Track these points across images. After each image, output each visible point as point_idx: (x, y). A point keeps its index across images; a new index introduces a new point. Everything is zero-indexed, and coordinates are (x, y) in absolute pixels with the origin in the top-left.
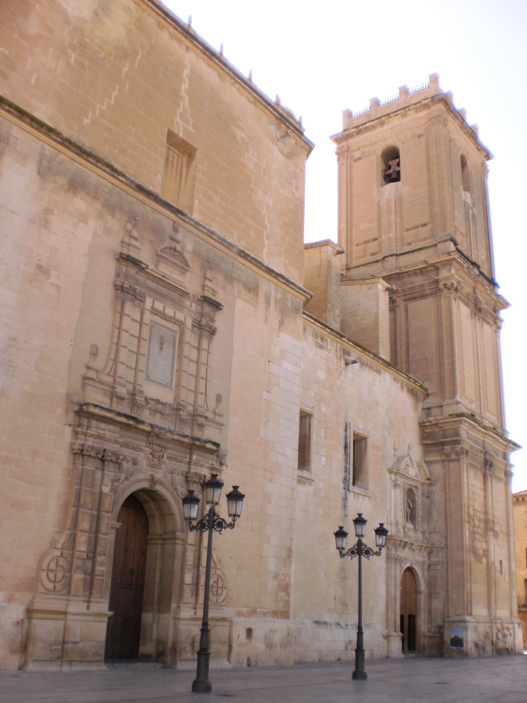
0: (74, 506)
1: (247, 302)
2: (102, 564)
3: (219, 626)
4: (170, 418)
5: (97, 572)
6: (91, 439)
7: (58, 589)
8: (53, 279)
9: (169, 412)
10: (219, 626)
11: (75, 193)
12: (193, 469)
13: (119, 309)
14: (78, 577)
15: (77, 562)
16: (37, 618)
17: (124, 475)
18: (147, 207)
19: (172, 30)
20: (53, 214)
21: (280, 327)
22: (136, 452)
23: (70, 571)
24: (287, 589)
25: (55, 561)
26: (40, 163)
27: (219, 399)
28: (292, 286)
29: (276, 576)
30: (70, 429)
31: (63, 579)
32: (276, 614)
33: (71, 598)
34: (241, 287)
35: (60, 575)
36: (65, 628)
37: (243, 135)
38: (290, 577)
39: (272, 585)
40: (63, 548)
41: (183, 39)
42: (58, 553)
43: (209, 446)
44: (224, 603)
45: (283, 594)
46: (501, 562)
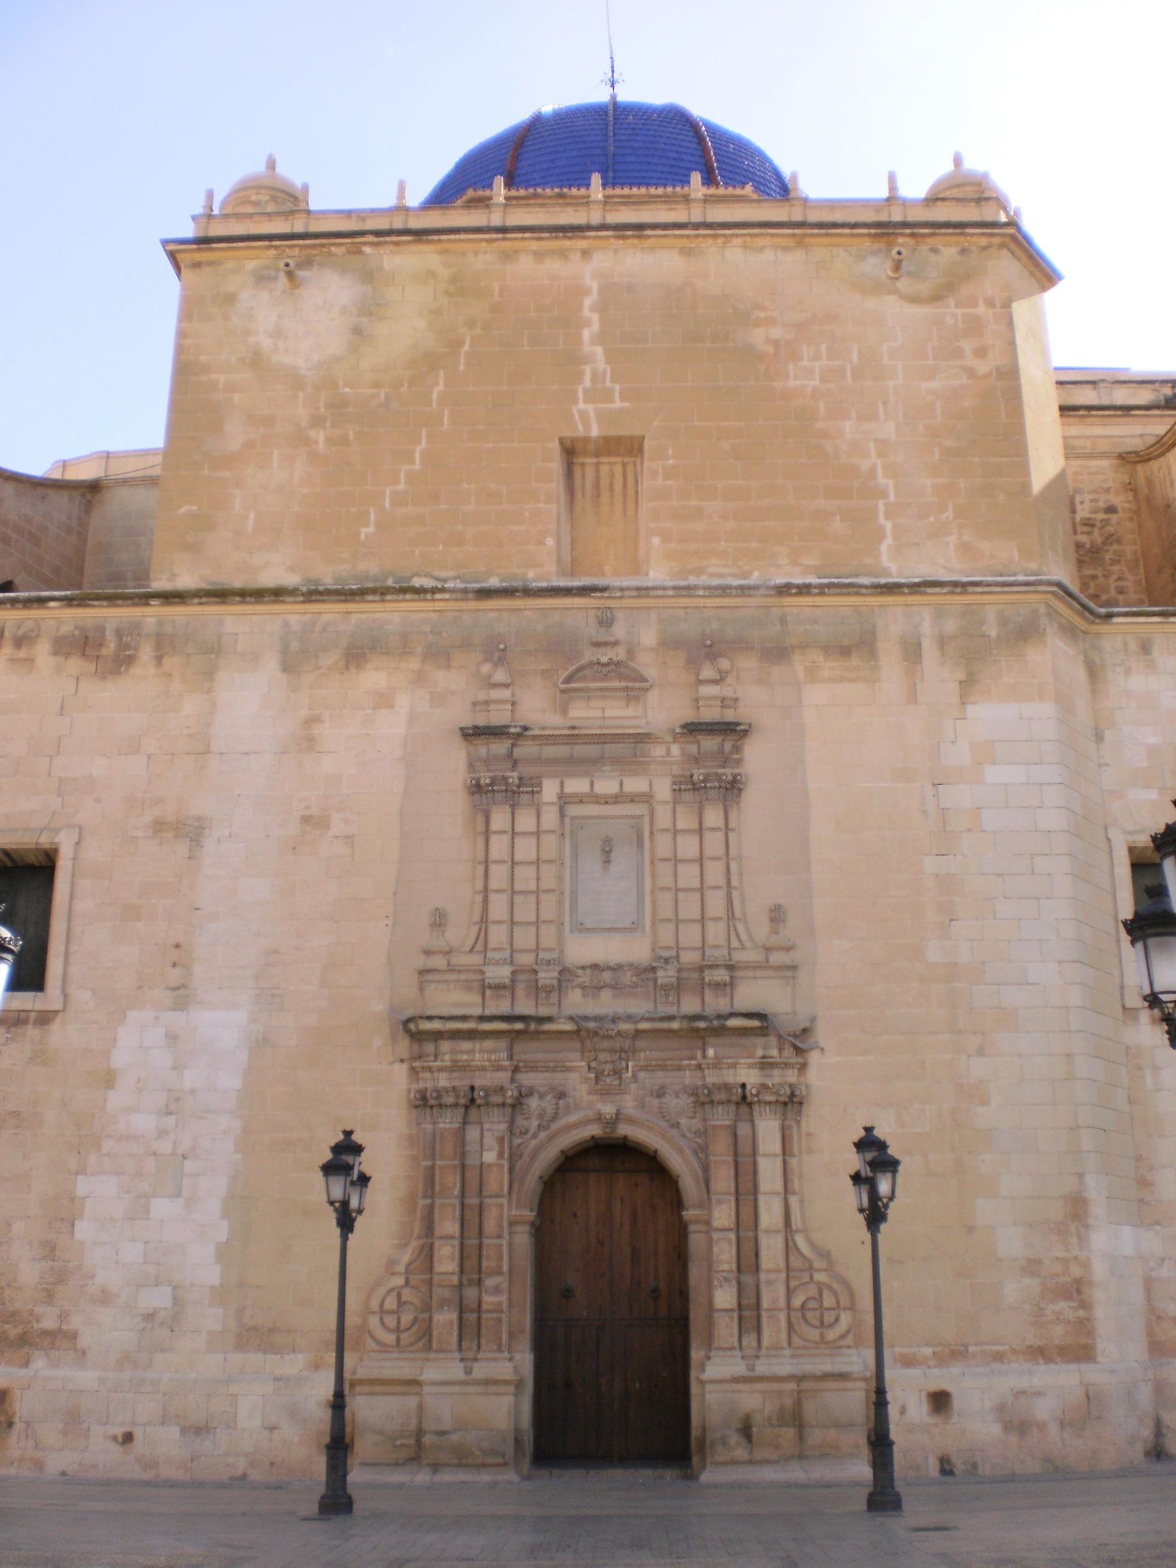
0: (424, 1197)
1: (842, 680)
2: (497, 1290)
3: (830, 1390)
4: (639, 989)
5: (484, 1307)
6: (443, 1075)
7: (403, 1342)
8: (337, 826)
9: (634, 979)
10: (830, 1390)
11: (359, 666)
12: (712, 1078)
13: (481, 827)
14: (445, 1318)
15: (439, 1293)
16: (361, 1394)
17: (535, 1123)
18: (527, 613)
19: (534, 245)
20: (323, 722)
22: (559, 1075)
23: (427, 1308)
24: (1079, 1292)
25: (394, 1294)
26: (285, 650)
27: (777, 915)
28: (980, 589)
29: (1032, 1267)
30: (405, 1067)
31: (413, 1324)
32: (1040, 1353)
33: (432, 1355)
34: (817, 657)
35: (406, 1319)
36: (421, 1408)
37: (776, 332)
38: (1086, 1264)
39: (1015, 1289)
40: (408, 1271)
41: (567, 243)
42: (399, 1281)
43: (733, 1022)
44: (849, 1341)
45: (1062, 1305)
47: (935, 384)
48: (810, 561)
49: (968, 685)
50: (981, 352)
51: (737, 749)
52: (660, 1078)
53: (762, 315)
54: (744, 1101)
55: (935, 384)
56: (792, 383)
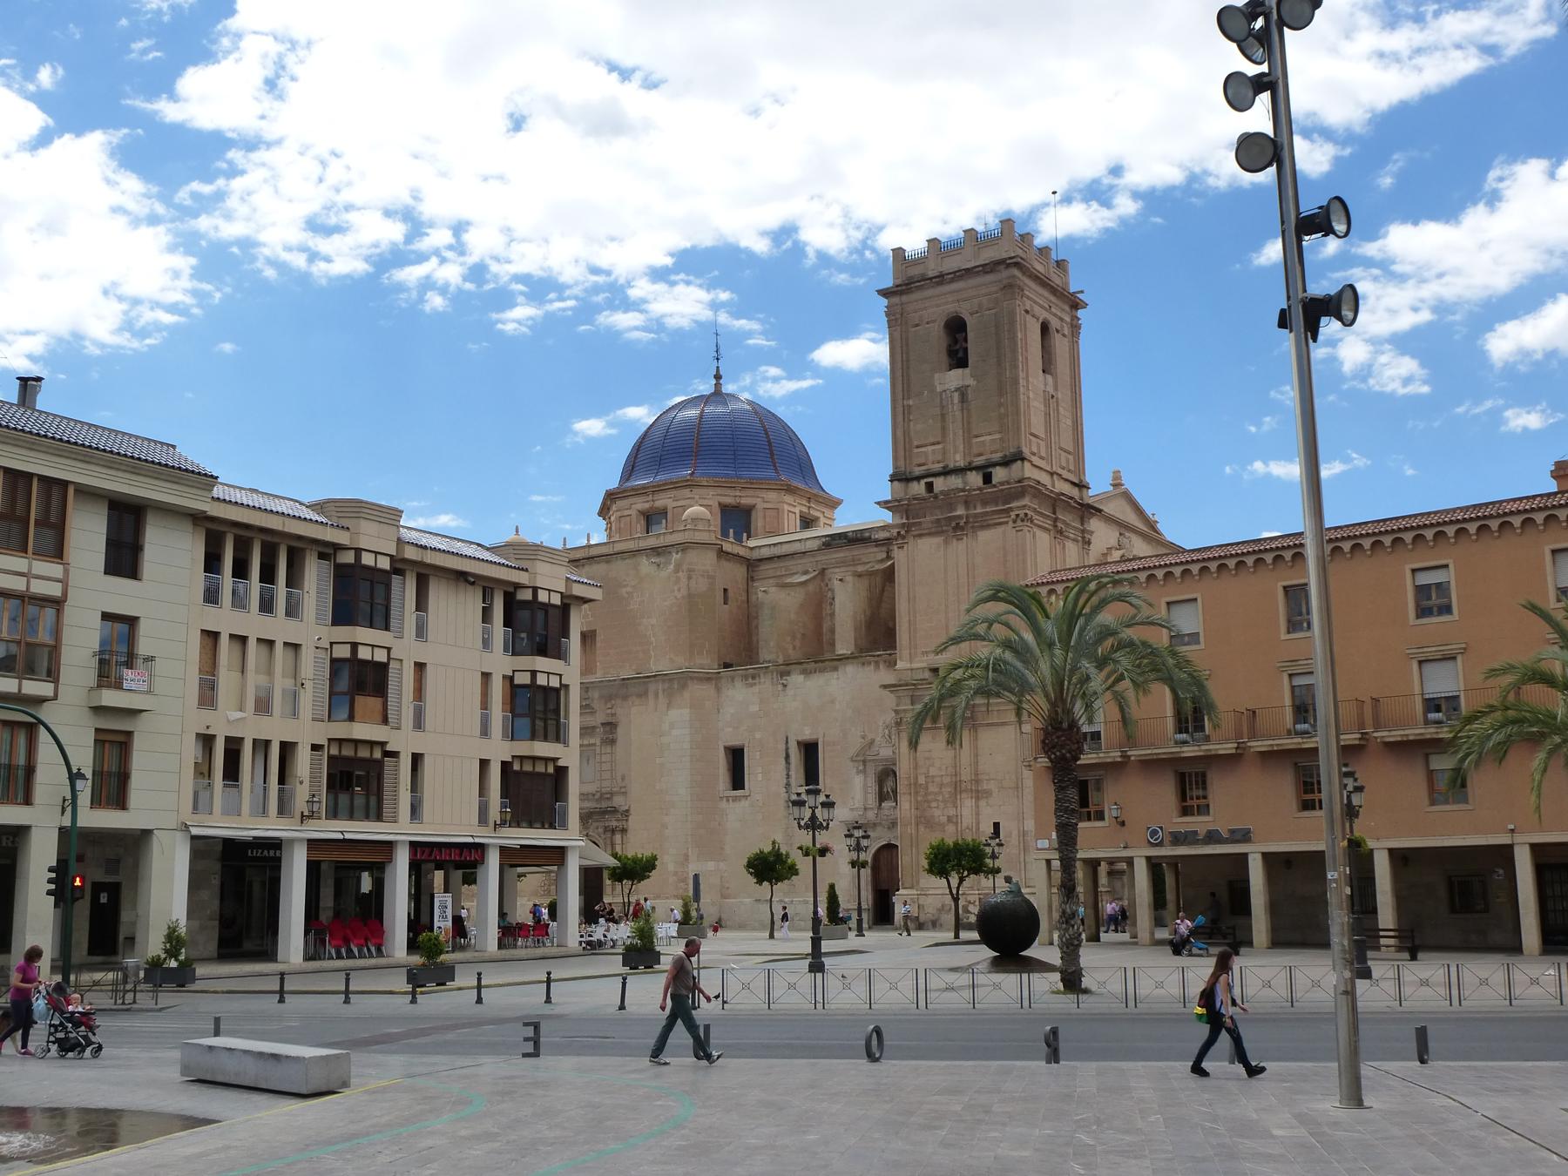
21: (668, 707)
27: (623, 779)
29: (676, 873)
37: (629, 589)
38: (688, 874)
45: (682, 884)
46: (997, 826)
47: (666, 603)
48: (634, 668)
49: (669, 706)
50: (679, 590)
51: (616, 729)
52: (597, 824)
53: (625, 583)
54: (613, 831)
55: (666, 603)
56: (632, 607)
